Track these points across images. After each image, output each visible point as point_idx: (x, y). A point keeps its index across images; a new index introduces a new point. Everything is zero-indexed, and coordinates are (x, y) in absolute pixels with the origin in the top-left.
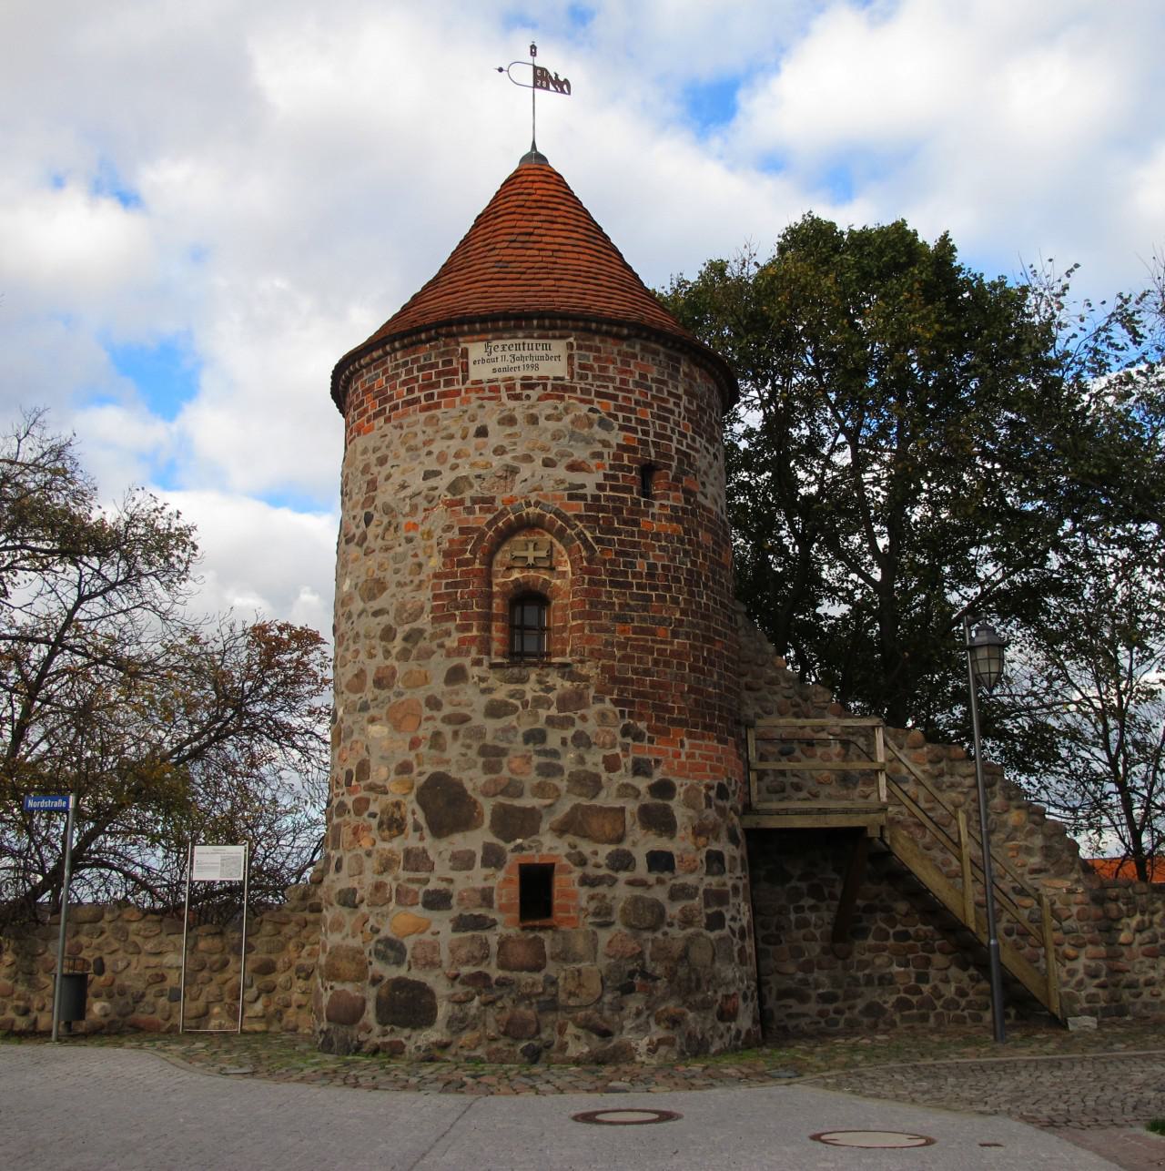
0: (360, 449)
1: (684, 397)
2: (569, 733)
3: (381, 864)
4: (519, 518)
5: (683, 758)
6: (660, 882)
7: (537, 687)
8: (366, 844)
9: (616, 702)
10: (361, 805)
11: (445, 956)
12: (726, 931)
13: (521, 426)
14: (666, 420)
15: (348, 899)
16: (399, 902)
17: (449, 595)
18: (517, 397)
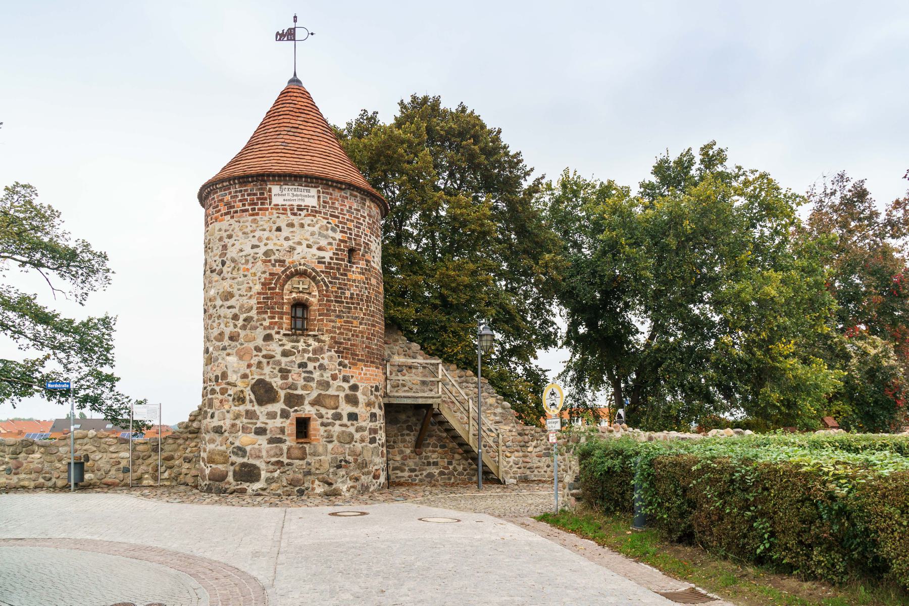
0: (217, 228)
1: (367, 217)
2: (317, 364)
4: (296, 270)
6: (352, 425)
7: (304, 345)
8: (227, 407)
9: (336, 352)
10: (223, 391)
11: (264, 453)
12: (376, 445)
13: (297, 228)
14: (359, 228)
15: (218, 430)
17: (265, 302)
18: (295, 214)
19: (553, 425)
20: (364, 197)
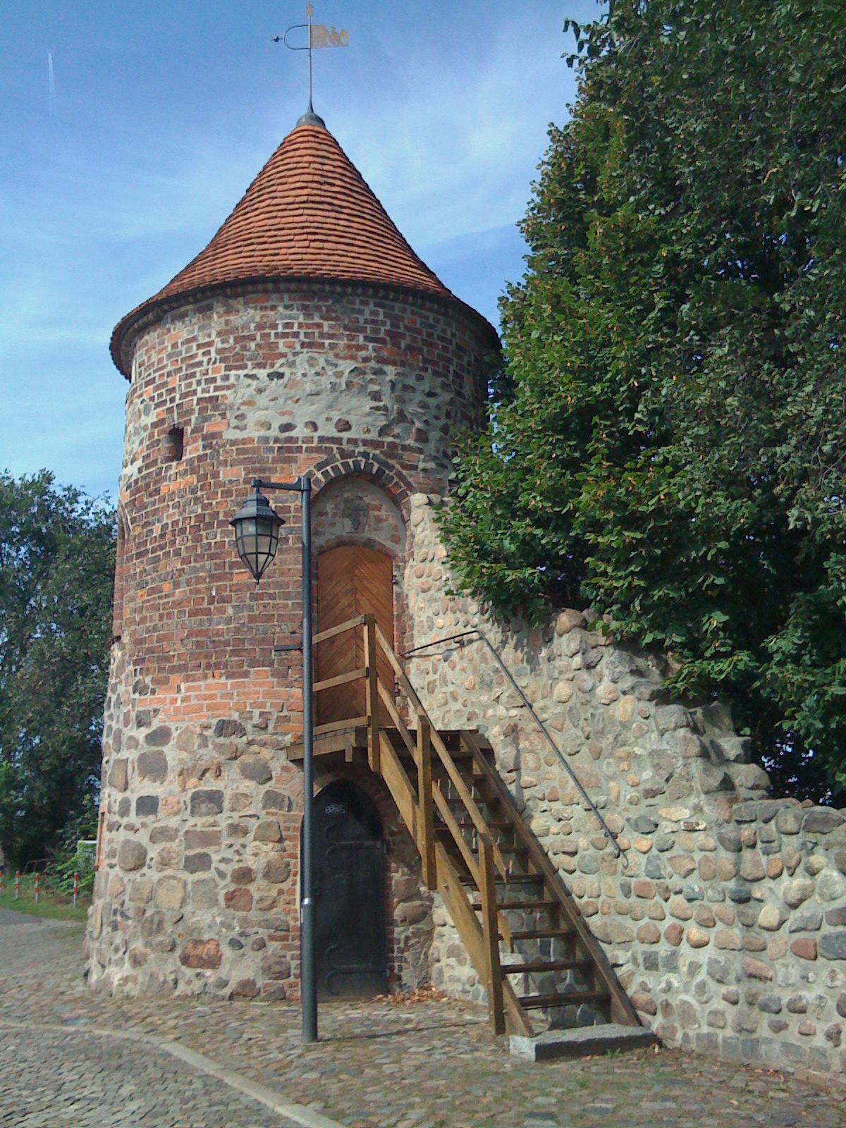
5: (179, 704)
20: (205, 303)
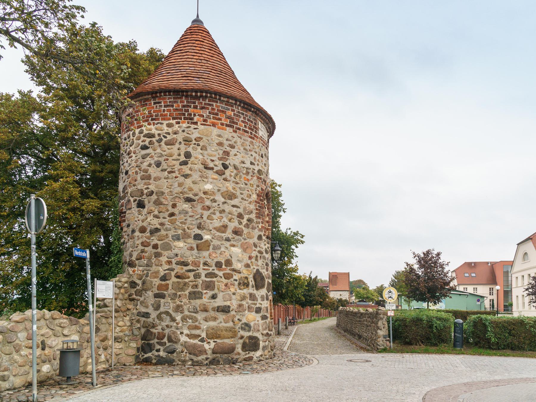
3: (241, 298)
8: (232, 290)
16: (248, 311)
19: (391, 307)
